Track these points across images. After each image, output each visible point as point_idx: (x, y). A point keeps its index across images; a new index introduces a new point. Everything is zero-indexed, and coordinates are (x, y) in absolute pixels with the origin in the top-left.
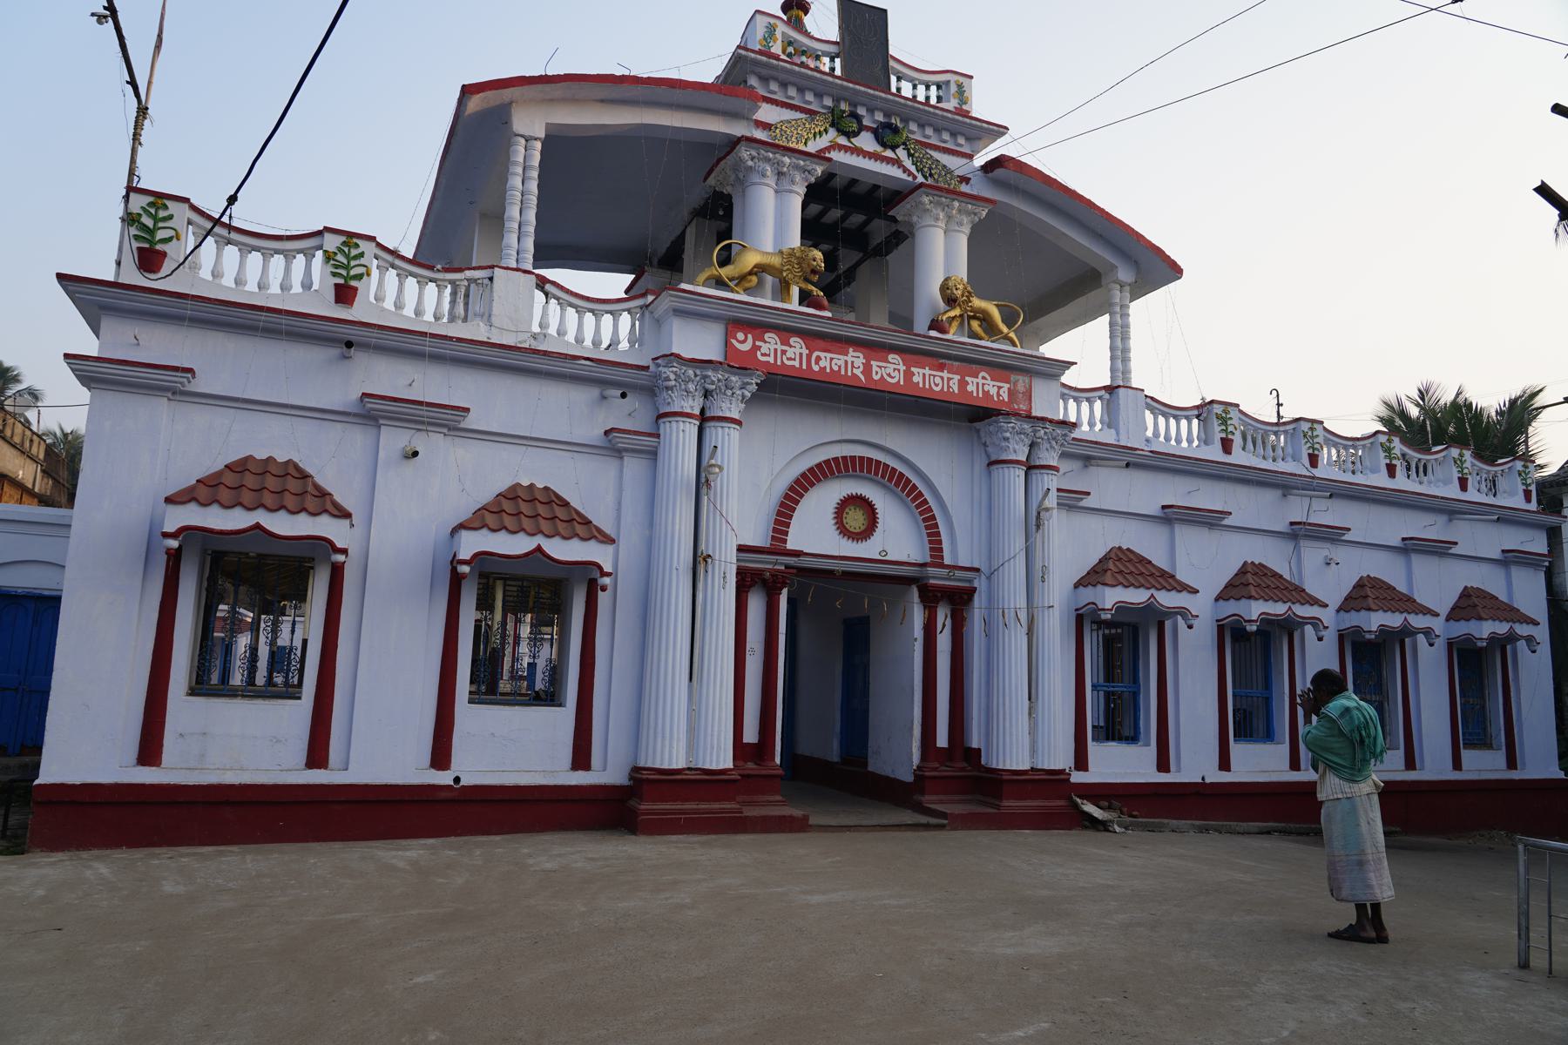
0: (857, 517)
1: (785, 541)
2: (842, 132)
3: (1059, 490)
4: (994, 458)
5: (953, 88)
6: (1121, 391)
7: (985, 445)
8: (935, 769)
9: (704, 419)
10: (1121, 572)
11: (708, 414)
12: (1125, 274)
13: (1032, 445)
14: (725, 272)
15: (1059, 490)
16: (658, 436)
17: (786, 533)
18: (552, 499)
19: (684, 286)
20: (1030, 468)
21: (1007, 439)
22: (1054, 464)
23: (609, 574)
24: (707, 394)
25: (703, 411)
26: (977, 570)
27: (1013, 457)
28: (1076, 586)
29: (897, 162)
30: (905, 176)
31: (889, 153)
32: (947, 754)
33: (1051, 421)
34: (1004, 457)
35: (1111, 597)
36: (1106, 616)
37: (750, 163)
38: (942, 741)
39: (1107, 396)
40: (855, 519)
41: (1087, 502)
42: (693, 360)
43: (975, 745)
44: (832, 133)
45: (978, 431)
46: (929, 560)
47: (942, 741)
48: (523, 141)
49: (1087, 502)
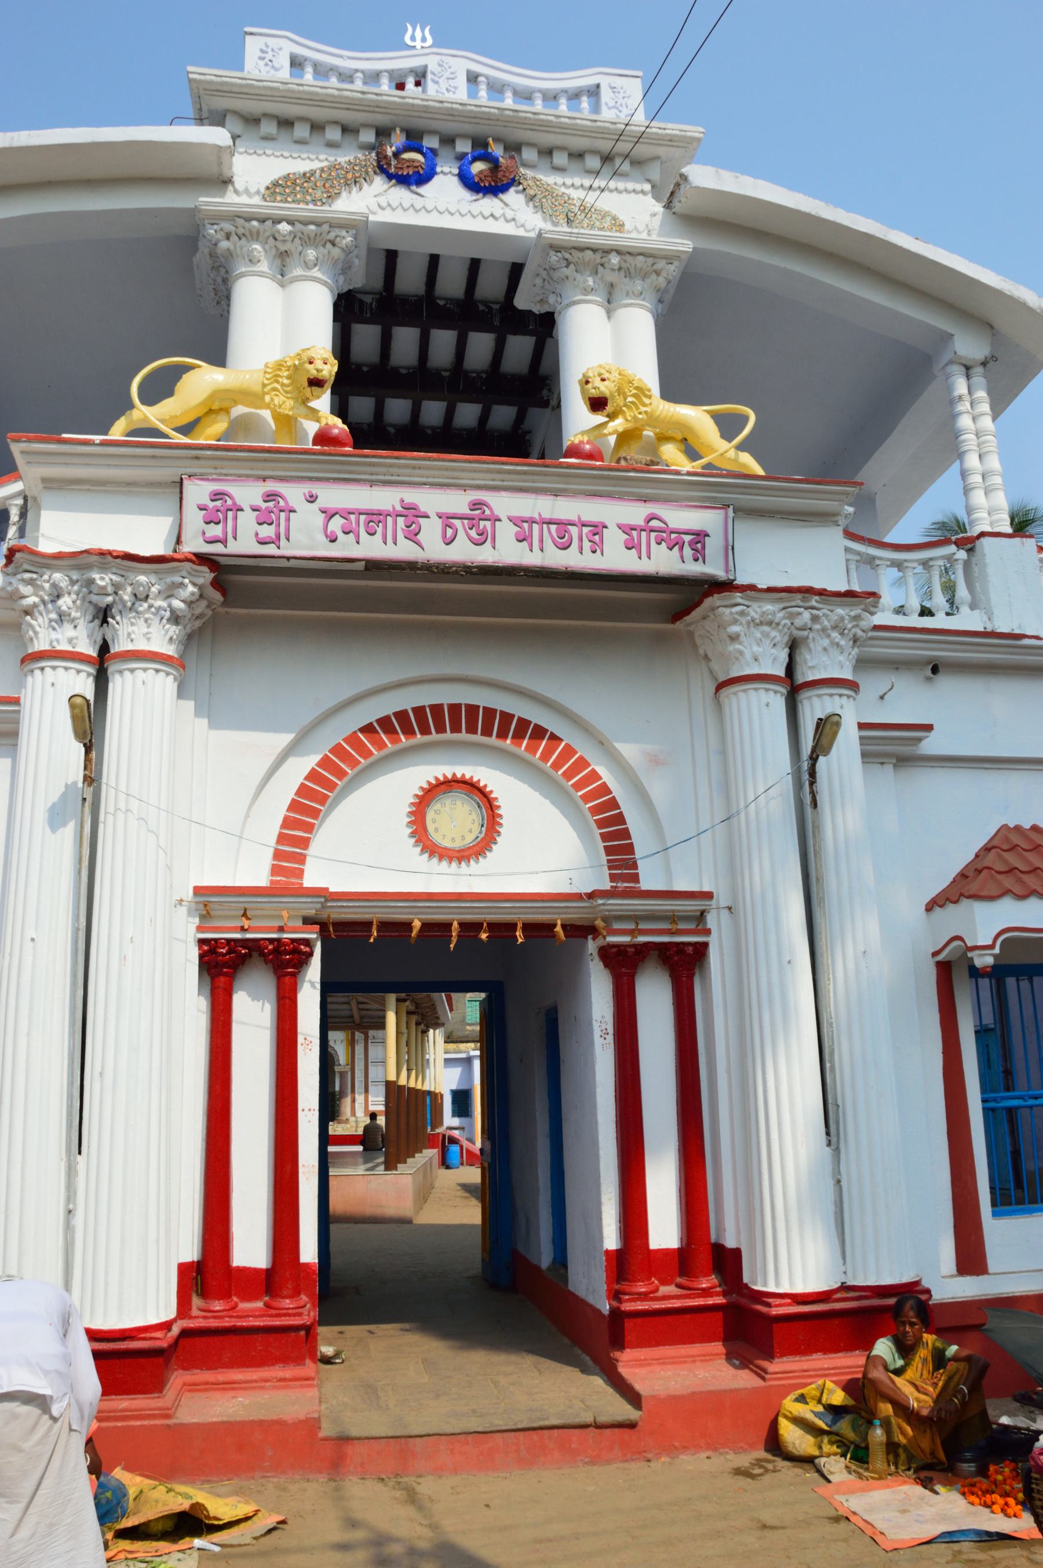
1: (300, 873)
3: (862, 726)
4: (722, 678)
5: (605, 95)
6: (986, 541)
7: (706, 657)
8: (644, 1297)
9: (103, 662)
10: (1012, 870)
12: (969, 346)
13: (793, 646)
15: (862, 726)
16: (16, 701)
17: (302, 859)
20: (793, 687)
21: (734, 638)
22: (847, 674)
24: (104, 615)
25: (104, 648)
26: (708, 896)
27: (754, 670)
28: (929, 908)
32: (680, 1263)
33: (822, 593)
34: (735, 673)
35: (987, 923)
36: (984, 960)
37: (224, 244)
38: (664, 1231)
39: (962, 555)
40: (455, 820)
41: (931, 745)
43: (730, 1243)
45: (691, 634)
46: (607, 885)
47: (664, 1231)
49: (931, 745)
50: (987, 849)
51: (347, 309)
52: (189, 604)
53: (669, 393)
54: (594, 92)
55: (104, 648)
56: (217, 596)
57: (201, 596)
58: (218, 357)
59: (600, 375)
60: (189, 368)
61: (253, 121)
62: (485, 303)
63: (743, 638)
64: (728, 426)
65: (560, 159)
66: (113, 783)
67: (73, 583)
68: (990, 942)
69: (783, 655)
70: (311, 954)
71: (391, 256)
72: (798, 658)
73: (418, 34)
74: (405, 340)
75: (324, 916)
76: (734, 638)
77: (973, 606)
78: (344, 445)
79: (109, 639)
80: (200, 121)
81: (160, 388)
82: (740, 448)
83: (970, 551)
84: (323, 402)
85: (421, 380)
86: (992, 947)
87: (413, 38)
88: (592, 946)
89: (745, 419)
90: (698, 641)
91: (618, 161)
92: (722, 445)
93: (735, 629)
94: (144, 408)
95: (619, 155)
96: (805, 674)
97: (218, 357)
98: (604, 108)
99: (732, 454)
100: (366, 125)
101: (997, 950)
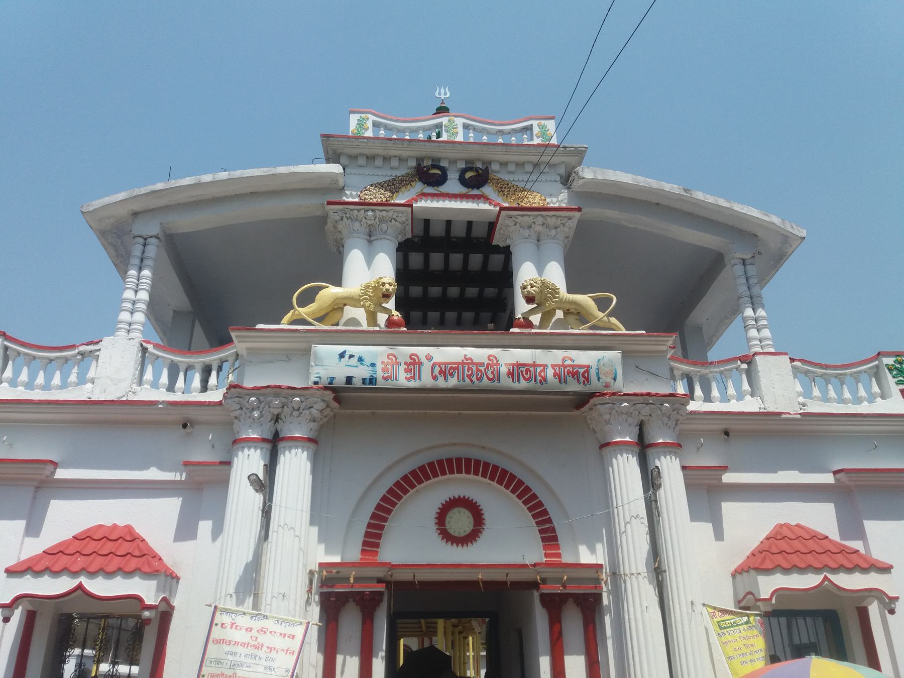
0: (461, 521)
2: (430, 184)
5: (536, 130)
6: (757, 358)
11: (281, 436)
14: (303, 311)
18: (129, 536)
19: (259, 326)
23: (150, 608)
25: (276, 434)
29: (486, 199)
30: (492, 208)
31: (475, 192)
35: (767, 585)
39: (745, 366)
40: (460, 521)
42: (255, 388)
44: (418, 187)
45: (585, 417)
48: (141, 240)
50: (768, 538)
51: (404, 249)
52: (321, 411)
53: (569, 292)
54: (529, 129)
55: (276, 434)
56: (336, 405)
57: (328, 406)
58: (338, 282)
59: (531, 284)
60: (322, 288)
61: (354, 157)
62: (477, 239)
63: (612, 421)
64: (602, 304)
65: (512, 167)
66: (278, 503)
67: (260, 402)
68: (768, 597)
69: (636, 430)
70: (381, 600)
71: (427, 222)
72: (645, 430)
73: (442, 91)
74: (437, 260)
75: (389, 579)
76: (608, 422)
77: (752, 395)
78: (400, 326)
79: (279, 429)
80: (328, 160)
81: (308, 298)
82: (609, 315)
83: (749, 363)
84: (391, 304)
85: (446, 277)
86: (770, 599)
87: (440, 94)
88: (536, 594)
89: (612, 300)
90: (589, 422)
91: (542, 167)
92: (601, 315)
93: (607, 417)
94: (301, 310)
95: (544, 163)
96: (649, 440)
97: (337, 281)
98: (535, 137)
99: (605, 318)
100: (410, 157)
101: (774, 601)
